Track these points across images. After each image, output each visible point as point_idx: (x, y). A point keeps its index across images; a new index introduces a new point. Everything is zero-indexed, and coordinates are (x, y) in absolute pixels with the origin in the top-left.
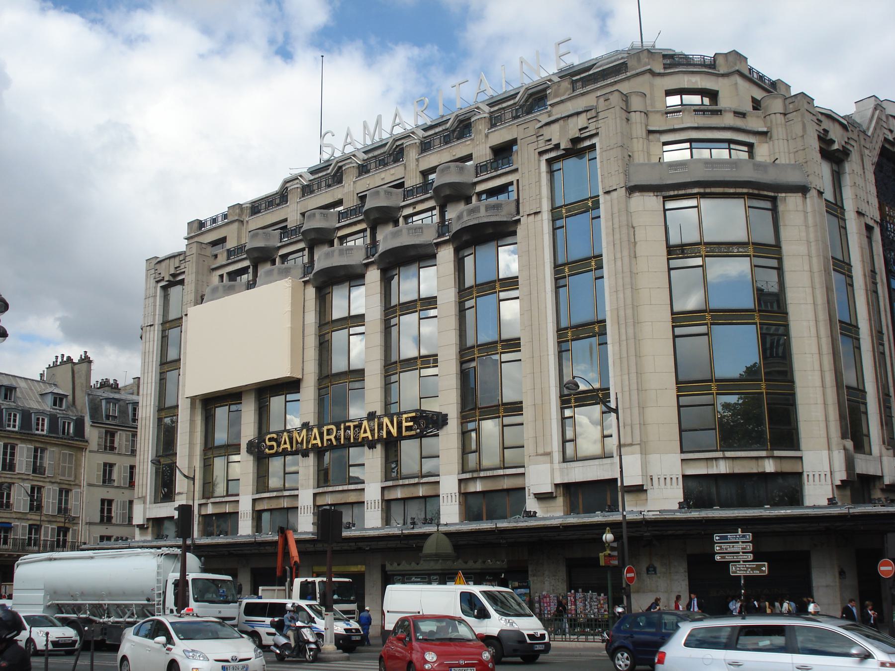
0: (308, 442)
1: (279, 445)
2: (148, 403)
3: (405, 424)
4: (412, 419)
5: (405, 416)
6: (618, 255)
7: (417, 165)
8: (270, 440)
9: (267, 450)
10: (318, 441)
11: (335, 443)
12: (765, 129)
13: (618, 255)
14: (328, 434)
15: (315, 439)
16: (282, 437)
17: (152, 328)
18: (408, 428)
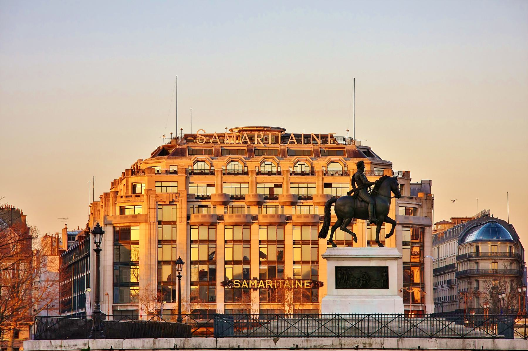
0: (258, 285)
1: (241, 285)
2: (154, 258)
3: (305, 284)
4: (308, 283)
5: (305, 281)
6: (392, 243)
7: (289, 180)
8: (236, 282)
9: (234, 286)
10: (263, 285)
11: (272, 287)
12: (421, 204)
13: (392, 243)
14: (268, 283)
15: (261, 284)
16: (243, 282)
17: (154, 223)
18: (307, 286)
